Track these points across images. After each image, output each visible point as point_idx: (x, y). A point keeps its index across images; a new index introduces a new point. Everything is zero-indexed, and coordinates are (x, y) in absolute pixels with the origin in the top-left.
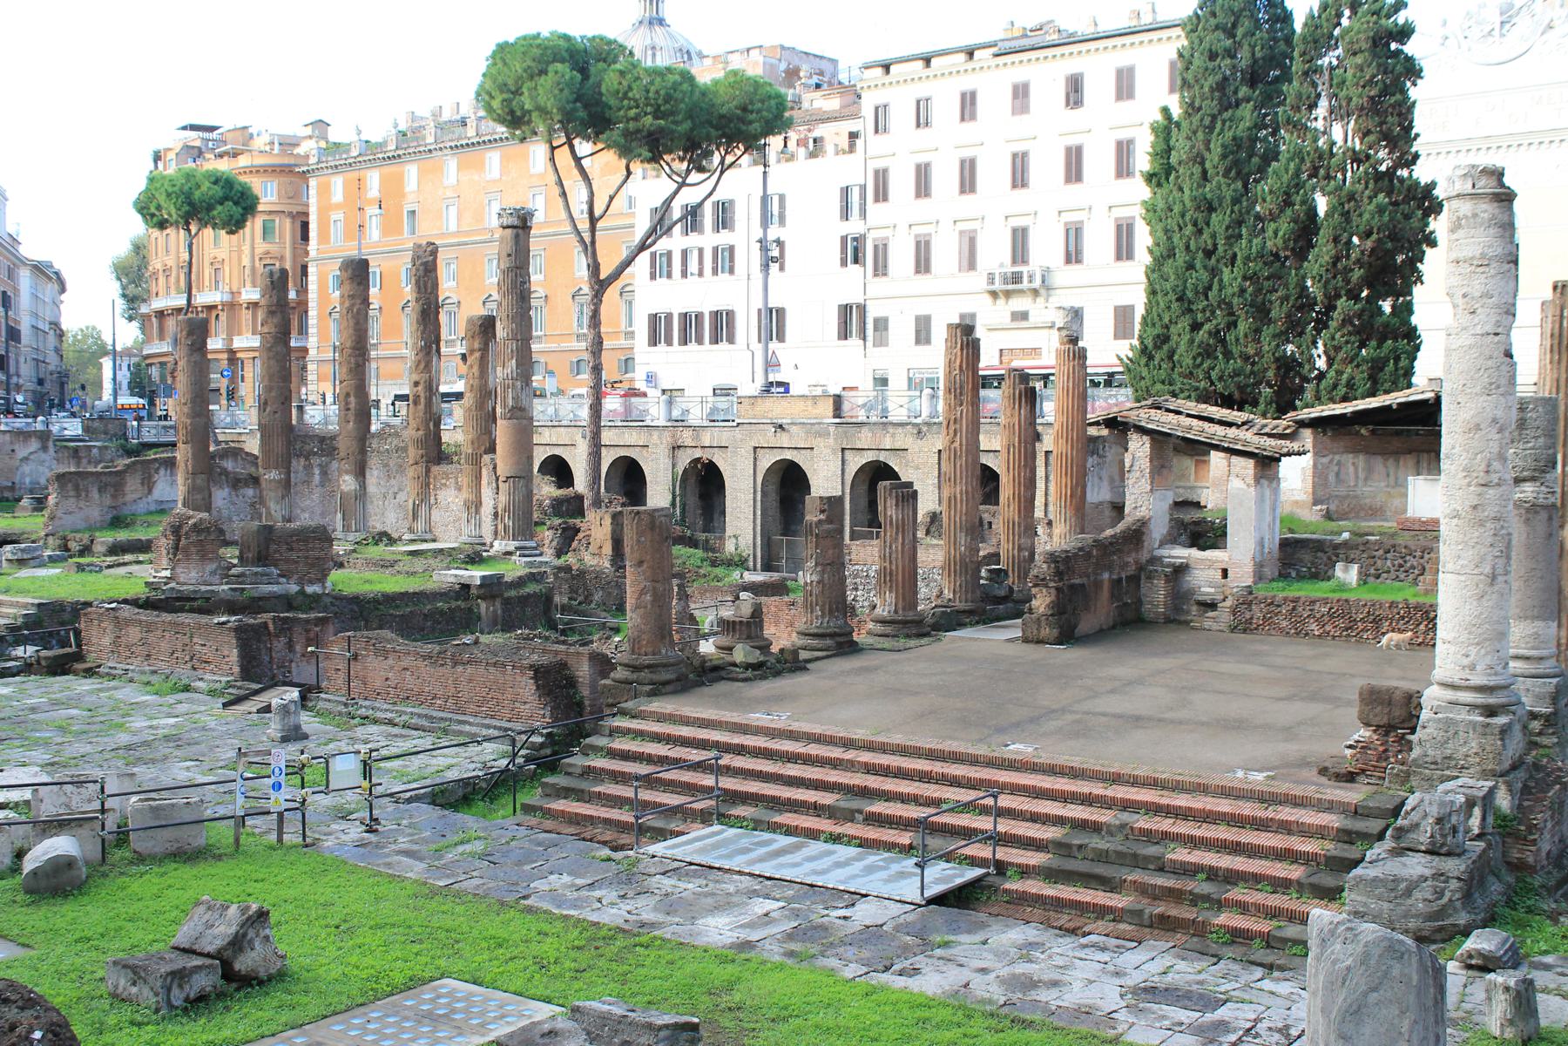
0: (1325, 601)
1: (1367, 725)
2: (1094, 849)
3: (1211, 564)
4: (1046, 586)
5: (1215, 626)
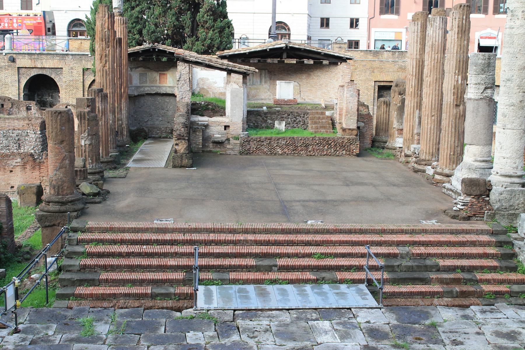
0: (284, 139)
1: (469, 195)
2: (406, 266)
3: (219, 124)
4: (184, 139)
5: (232, 153)
